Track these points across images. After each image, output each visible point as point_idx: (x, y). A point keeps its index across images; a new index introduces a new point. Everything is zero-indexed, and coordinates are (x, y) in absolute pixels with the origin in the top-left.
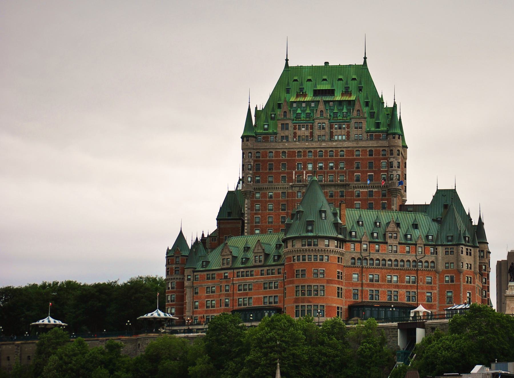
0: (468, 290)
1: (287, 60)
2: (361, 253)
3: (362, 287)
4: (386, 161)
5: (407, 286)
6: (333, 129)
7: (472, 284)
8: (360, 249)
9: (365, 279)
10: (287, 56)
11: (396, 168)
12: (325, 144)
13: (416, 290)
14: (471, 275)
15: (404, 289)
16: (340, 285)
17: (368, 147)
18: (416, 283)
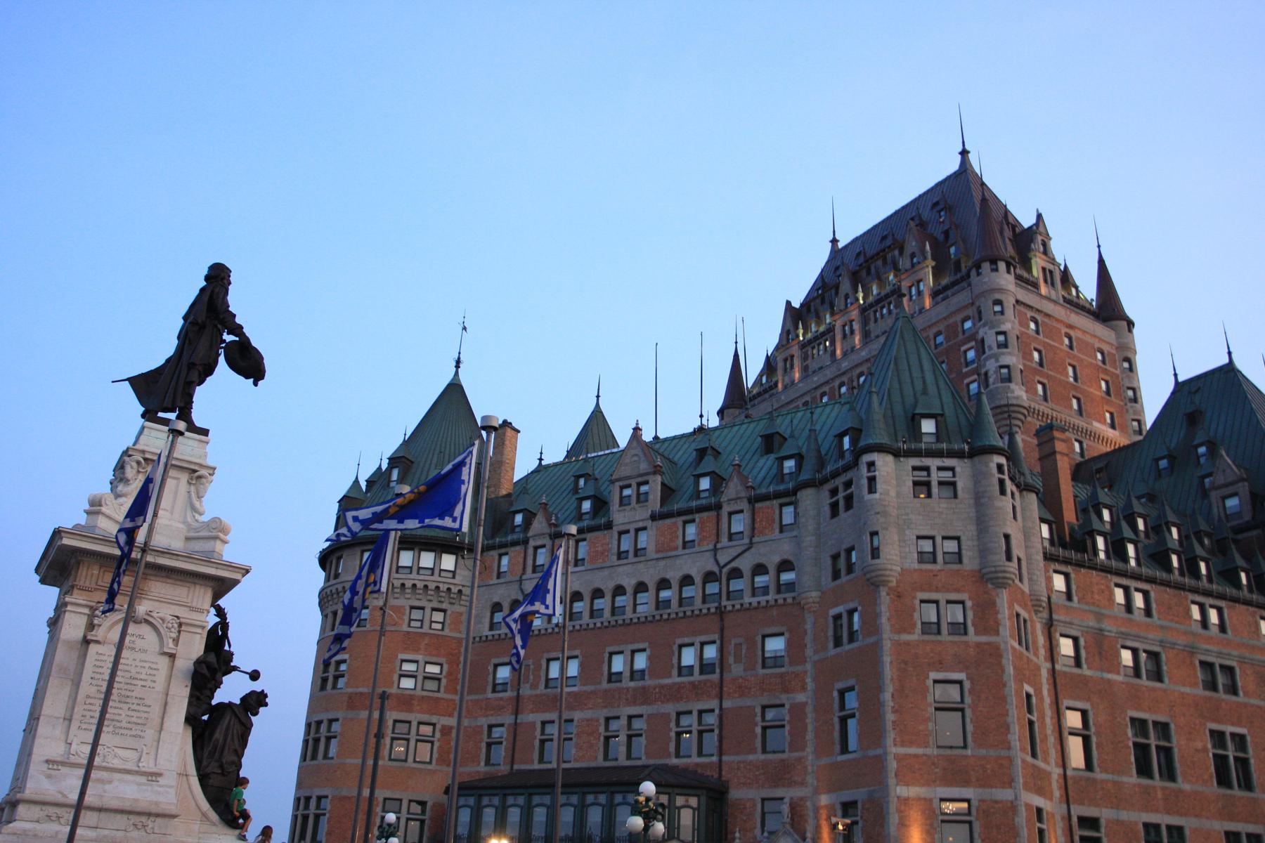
0: (940, 665)
1: (834, 241)
2: (521, 581)
3: (517, 713)
4: (973, 343)
5: (680, 687)
6: (869, 324)
7: (972, 637)
8: (521, 568)
9: (531, 681)
10: (834, 234)
11: (995, 349)
12: (846, 364)
13: (714, 704)
14: (957, 590)
15: (668, 701)
16: (410, 711)
17: (929, 327)
18: (718, 670)
